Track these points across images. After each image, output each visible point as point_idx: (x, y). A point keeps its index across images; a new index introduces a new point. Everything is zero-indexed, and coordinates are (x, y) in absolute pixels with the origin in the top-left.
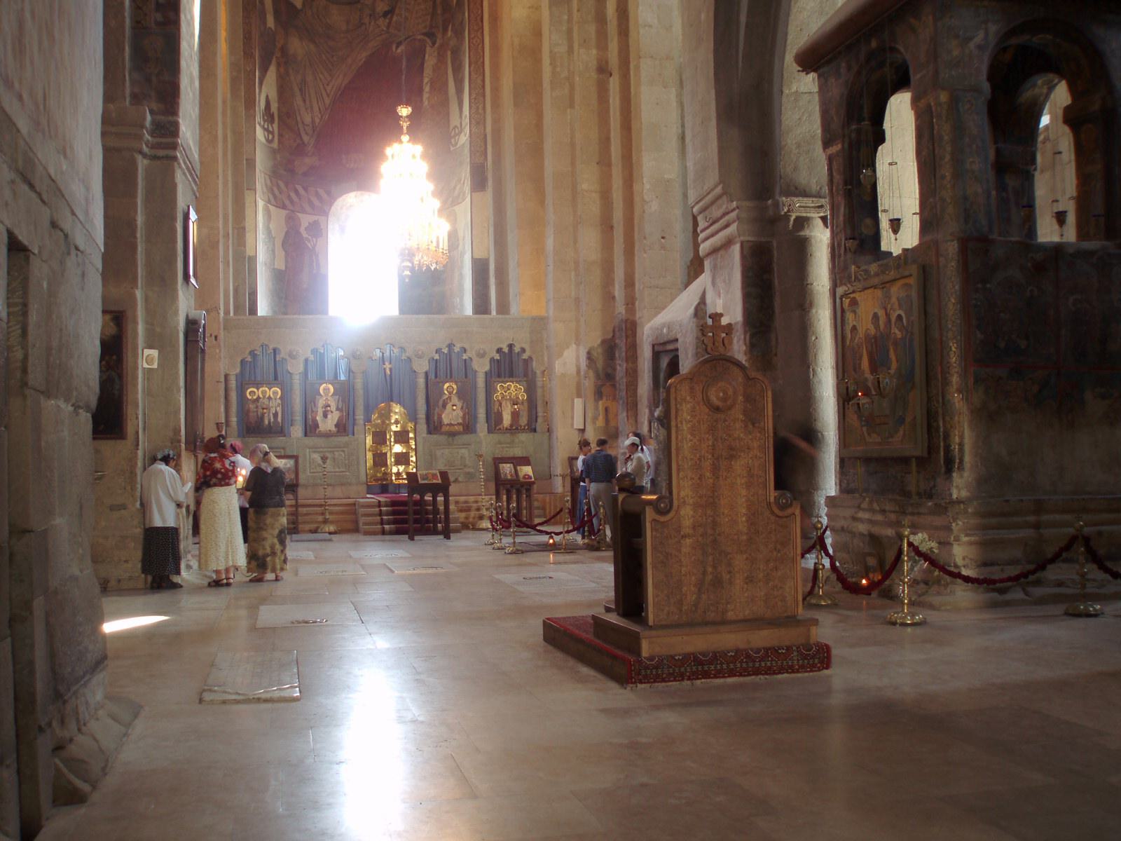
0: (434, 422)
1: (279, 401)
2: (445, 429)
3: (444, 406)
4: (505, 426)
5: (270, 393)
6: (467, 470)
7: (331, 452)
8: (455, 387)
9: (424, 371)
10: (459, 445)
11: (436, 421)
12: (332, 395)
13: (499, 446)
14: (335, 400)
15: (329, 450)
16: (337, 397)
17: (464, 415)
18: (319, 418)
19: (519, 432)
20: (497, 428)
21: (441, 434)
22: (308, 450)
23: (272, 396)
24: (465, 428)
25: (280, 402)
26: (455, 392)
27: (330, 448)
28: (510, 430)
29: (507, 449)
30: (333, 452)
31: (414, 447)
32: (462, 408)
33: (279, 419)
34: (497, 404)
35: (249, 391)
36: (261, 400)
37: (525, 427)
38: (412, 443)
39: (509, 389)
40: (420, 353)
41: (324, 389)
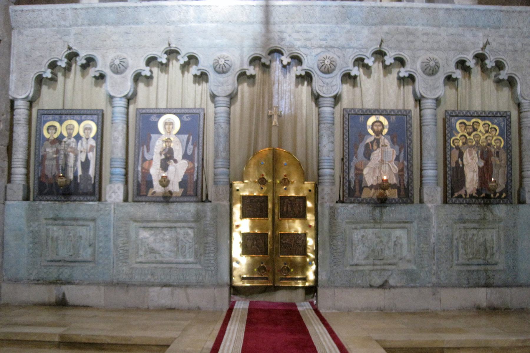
0: (350, 182)
1: (93, 143)
2: (367, 194)
3: (368, 155)
4: (469, 191)
5: (78, 128)
6: (404, 266)
7: (171, 228)
8: (385, 122)
9: (333, 94)
10: (391, 222)
11: (353, 181)
12: (179, 133)
13: (462, 226)
14: (181, 141)
15: (169, 225)
16: (186, 136)
17: (401, 171)
18: (155, 171)
19: (492, 204)
20: (456, 195)
21: (361, 202)
22: (133, 225)
23: (82, 134)
24: (402, 193)
25: (94, 144)
26: (385, 131)
27: (168, 221)
28: (474, 197)
29: (475, 232)
30: (175, 227)
31: (312, 224)
32: (397, 159)
33: (91, 172)
34: (456, 153)
35: (47, 124)
36: (65, 140)
37: (501, 193)
38: (310, 217)
39: (475, 130)
40: (327, 62)
41: (166, 124)
